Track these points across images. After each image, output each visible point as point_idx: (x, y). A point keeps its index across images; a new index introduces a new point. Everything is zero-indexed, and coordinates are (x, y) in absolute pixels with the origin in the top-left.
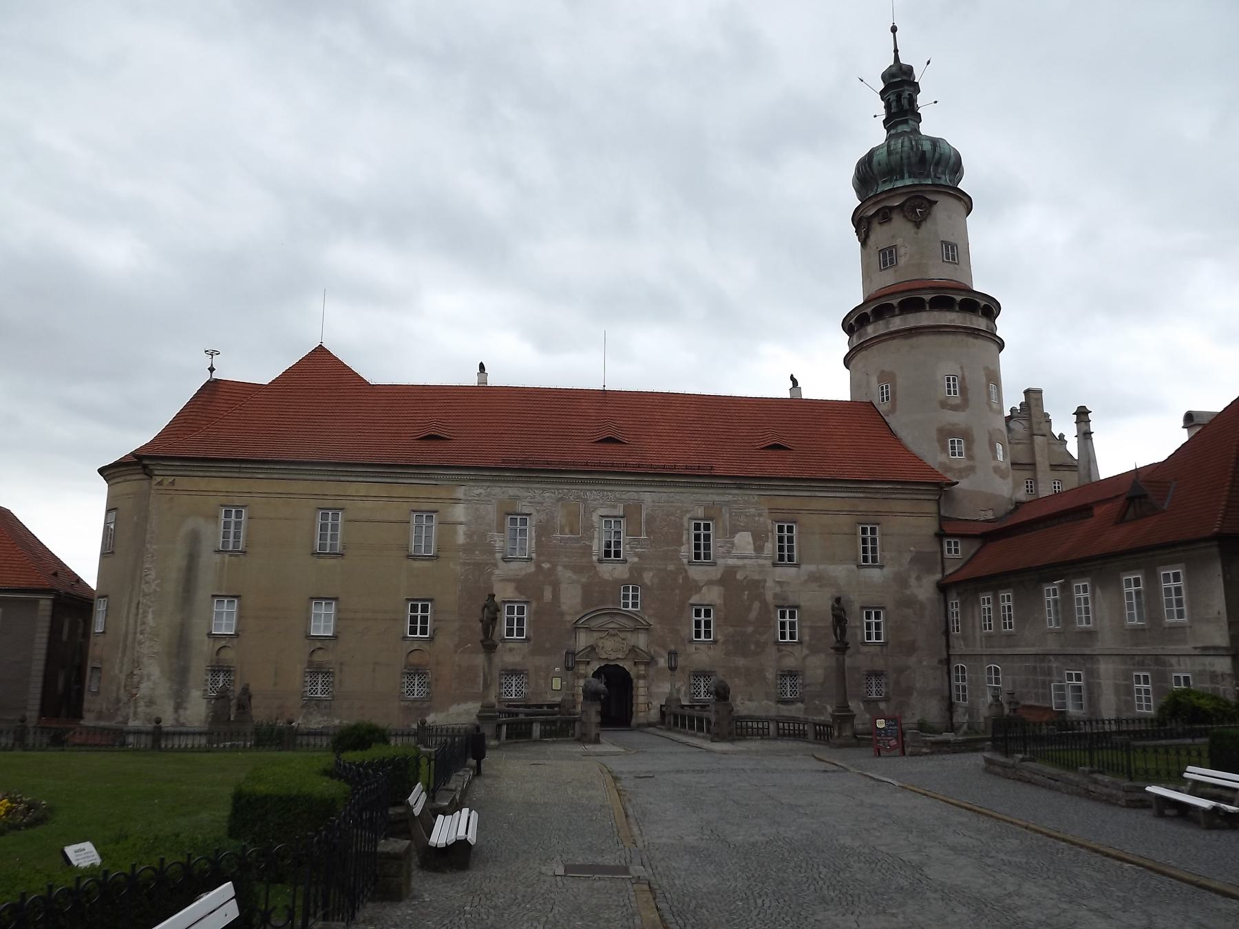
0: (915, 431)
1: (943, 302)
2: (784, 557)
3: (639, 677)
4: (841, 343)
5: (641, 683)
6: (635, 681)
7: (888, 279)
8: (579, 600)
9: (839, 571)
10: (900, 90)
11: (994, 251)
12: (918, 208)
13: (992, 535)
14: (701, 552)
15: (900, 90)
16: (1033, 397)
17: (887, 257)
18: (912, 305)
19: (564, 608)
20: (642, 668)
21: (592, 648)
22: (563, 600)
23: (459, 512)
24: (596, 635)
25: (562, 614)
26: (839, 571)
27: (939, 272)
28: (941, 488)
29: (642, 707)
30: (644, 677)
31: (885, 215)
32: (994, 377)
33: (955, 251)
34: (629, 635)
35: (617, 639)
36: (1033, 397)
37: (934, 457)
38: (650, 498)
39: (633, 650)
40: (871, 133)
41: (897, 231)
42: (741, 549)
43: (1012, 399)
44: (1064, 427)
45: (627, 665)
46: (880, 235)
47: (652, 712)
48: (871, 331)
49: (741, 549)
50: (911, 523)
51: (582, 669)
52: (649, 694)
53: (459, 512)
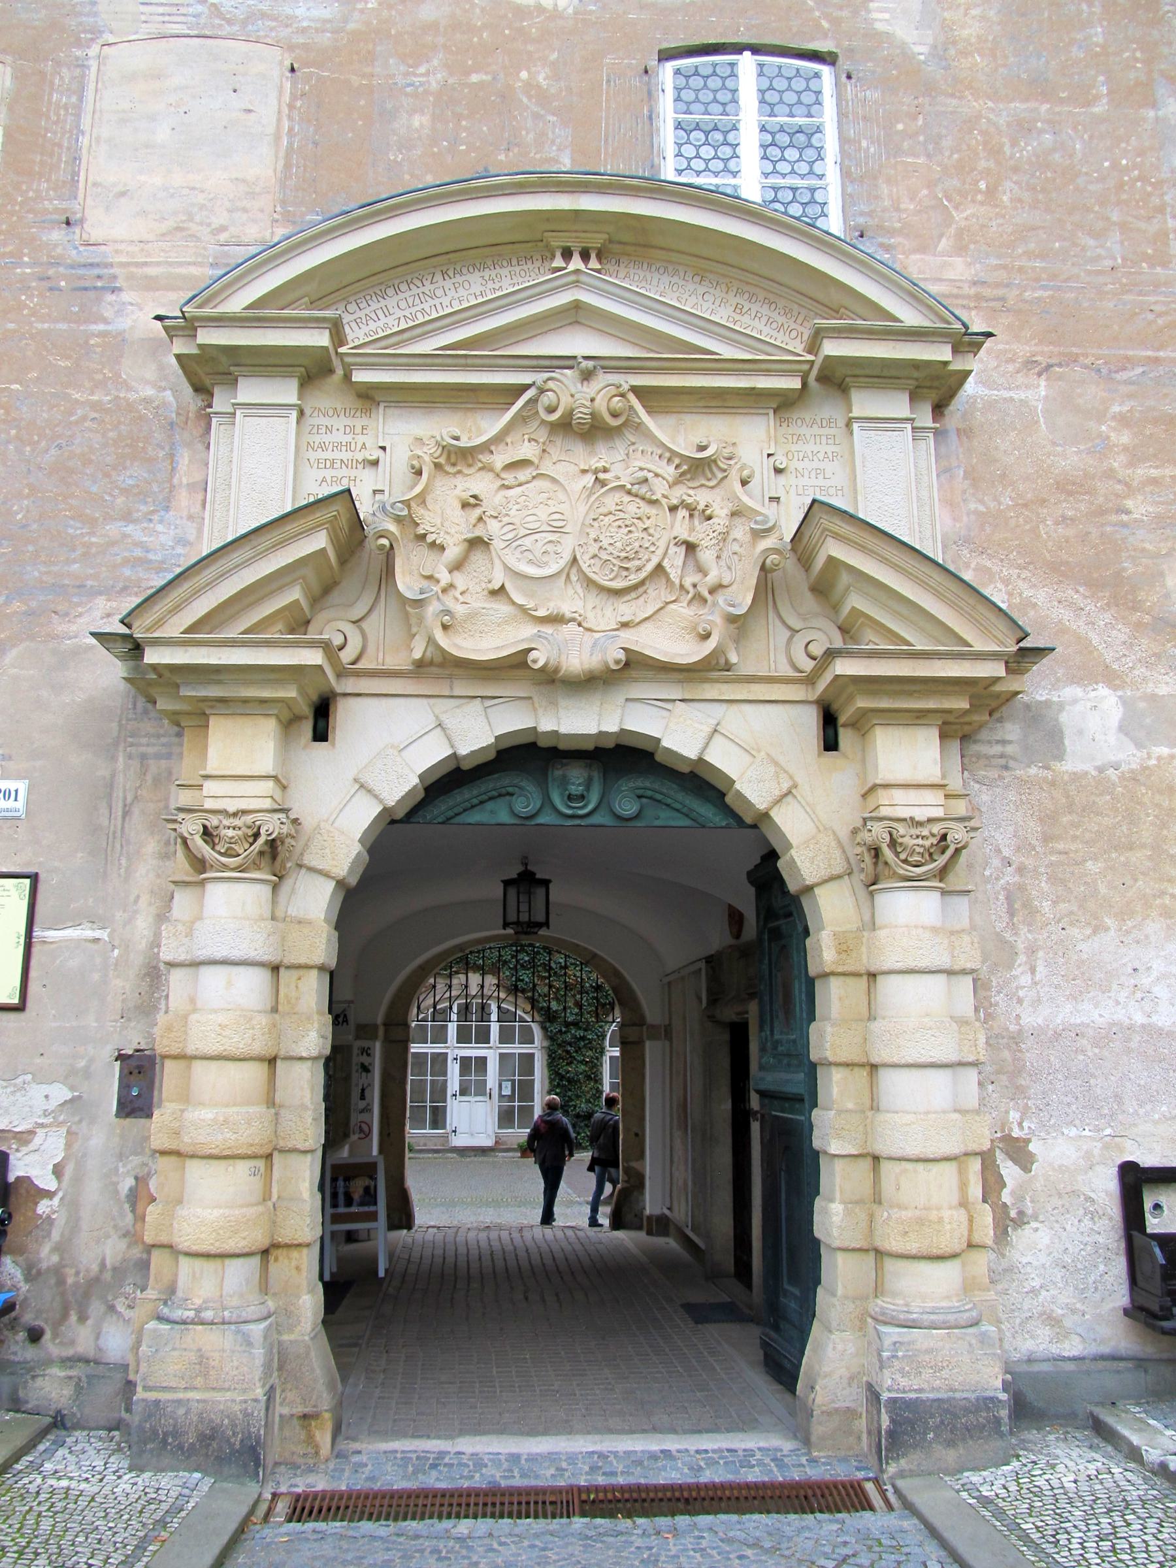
3: (878, 863)
5: (909, 911)
6: (832, 913)
8: (260, 164)
19: (112, 228)
20: (907, 757)
21: (352, 551)
22: (102, 167)
24: (405, 436)
25: (94, 283)
29: (931, 1199)
30: (940, 859)
34: (749, 440)
35: (619, 461)
39: (810, 569)
45: (752, 746)
47: (1034, 1246)
51: (239, 763)
52: (1001, 1061)
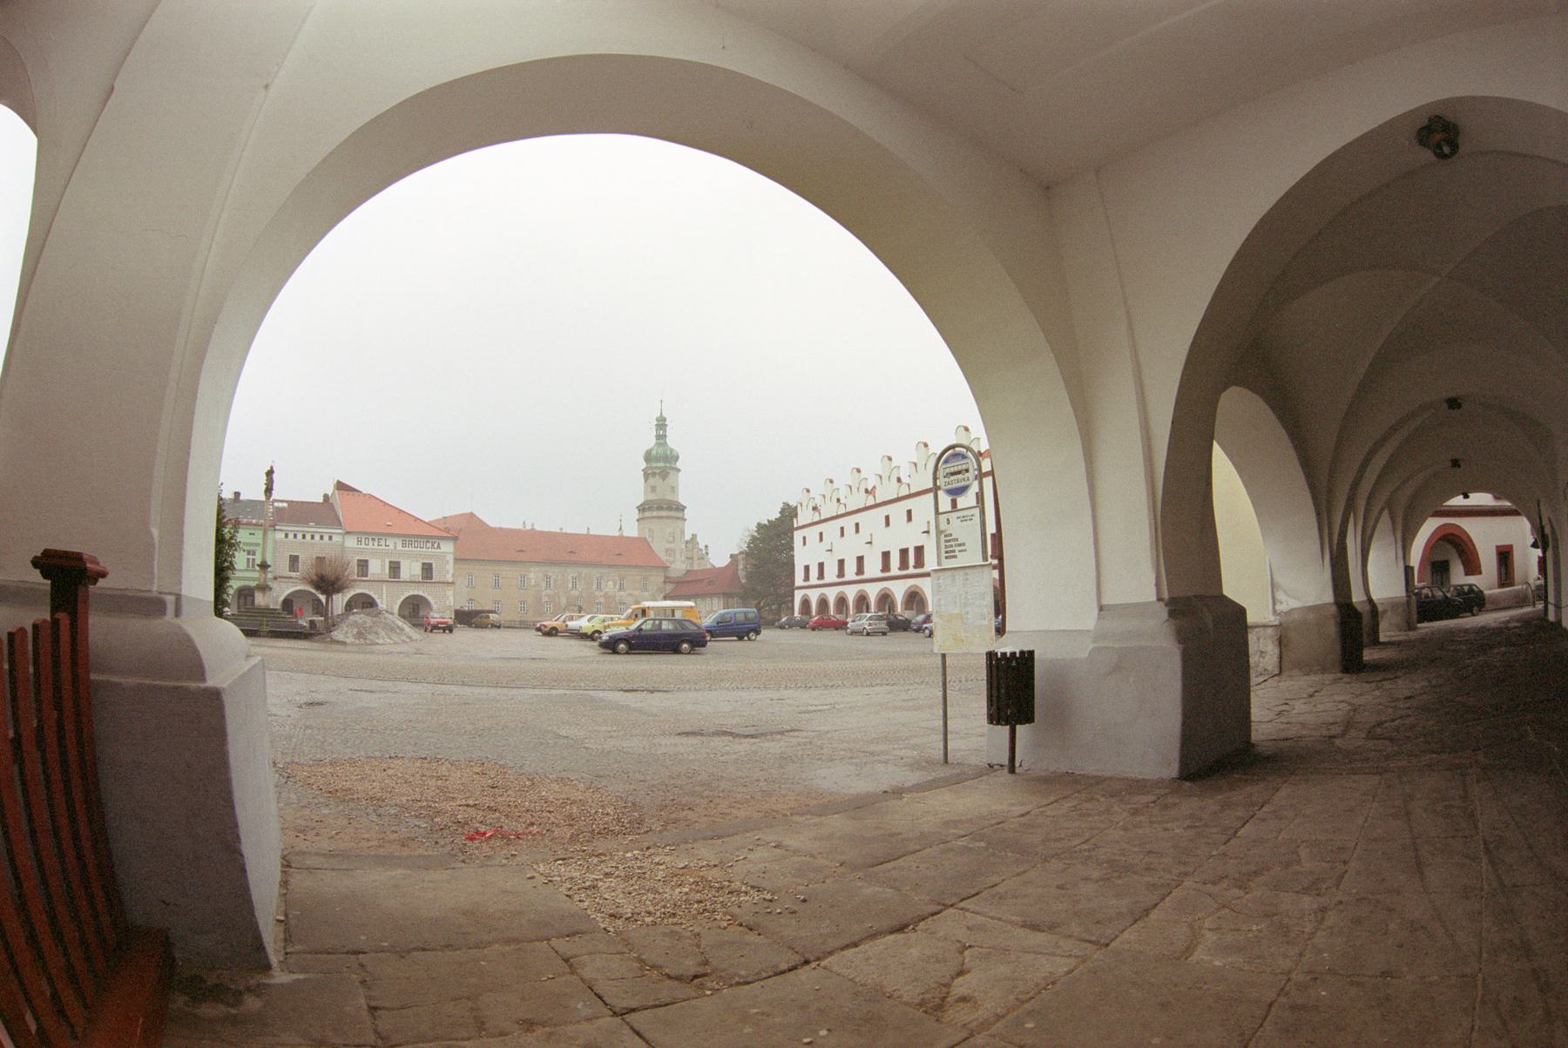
0: (659, 547)
1: (669, 508)
2: (621, 589)
4: (636, 515)
7: (652, 497)
9: (637, 593)
10: (661, 424)
11: (687, 488)
12: (664, 474)
13: (679, 582)
14: (599, 584)
15: (661, 424)
16: (694, 536)
17: (653, 489)
18: (660, 508)
23: (532, 575)
26: (637, 593)
27: (669, 497)
28: (666, 568)
31: (654, 474)
32: (683, 532)
33: (673, 489)
36: (694, 536)
37: (664, 558)
38: (585, 571)
40: (650, 442)
41: (656, 481)
42: (610, 587)
43: (688, 537)
44: (702, 546)
46: (651, 481)
48: (647, 514)
49: (610, 587)
50: (657, 579)
53: (532, 575)
